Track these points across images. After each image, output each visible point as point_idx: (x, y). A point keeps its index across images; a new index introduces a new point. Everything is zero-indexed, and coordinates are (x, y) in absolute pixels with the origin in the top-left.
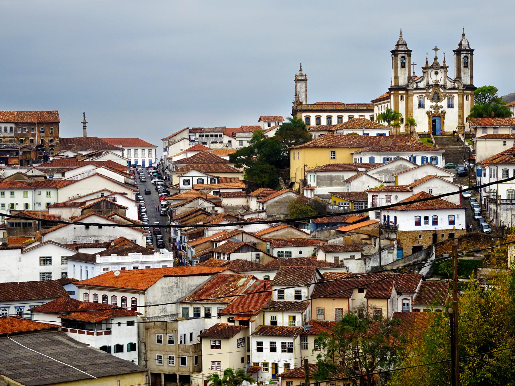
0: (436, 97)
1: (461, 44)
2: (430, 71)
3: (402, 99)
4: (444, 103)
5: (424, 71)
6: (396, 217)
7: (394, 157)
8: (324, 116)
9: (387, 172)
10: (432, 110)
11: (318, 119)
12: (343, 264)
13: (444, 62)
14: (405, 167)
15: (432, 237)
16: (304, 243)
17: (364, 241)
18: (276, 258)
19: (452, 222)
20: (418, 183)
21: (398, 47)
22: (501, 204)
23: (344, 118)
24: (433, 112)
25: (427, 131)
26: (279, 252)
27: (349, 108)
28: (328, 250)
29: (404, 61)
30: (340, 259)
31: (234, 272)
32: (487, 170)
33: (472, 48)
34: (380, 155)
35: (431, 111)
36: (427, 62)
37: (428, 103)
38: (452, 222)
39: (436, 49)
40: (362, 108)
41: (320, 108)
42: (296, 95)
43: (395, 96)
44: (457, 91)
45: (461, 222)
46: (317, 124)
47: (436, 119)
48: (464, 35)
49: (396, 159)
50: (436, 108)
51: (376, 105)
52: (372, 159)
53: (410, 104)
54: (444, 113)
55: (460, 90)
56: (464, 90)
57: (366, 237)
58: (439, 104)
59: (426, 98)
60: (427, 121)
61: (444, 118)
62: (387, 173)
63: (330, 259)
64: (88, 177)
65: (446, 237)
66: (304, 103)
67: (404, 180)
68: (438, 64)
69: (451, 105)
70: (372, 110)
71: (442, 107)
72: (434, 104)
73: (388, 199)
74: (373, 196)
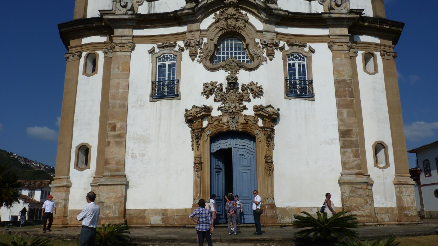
4: (270, 76)
10: (210, 102)
24: (216, 113)
35: (208, 110)
53: (113, 82)
58: (244, 77)
61: (270, 138)
71: (258, 92)
72: (220, 77)
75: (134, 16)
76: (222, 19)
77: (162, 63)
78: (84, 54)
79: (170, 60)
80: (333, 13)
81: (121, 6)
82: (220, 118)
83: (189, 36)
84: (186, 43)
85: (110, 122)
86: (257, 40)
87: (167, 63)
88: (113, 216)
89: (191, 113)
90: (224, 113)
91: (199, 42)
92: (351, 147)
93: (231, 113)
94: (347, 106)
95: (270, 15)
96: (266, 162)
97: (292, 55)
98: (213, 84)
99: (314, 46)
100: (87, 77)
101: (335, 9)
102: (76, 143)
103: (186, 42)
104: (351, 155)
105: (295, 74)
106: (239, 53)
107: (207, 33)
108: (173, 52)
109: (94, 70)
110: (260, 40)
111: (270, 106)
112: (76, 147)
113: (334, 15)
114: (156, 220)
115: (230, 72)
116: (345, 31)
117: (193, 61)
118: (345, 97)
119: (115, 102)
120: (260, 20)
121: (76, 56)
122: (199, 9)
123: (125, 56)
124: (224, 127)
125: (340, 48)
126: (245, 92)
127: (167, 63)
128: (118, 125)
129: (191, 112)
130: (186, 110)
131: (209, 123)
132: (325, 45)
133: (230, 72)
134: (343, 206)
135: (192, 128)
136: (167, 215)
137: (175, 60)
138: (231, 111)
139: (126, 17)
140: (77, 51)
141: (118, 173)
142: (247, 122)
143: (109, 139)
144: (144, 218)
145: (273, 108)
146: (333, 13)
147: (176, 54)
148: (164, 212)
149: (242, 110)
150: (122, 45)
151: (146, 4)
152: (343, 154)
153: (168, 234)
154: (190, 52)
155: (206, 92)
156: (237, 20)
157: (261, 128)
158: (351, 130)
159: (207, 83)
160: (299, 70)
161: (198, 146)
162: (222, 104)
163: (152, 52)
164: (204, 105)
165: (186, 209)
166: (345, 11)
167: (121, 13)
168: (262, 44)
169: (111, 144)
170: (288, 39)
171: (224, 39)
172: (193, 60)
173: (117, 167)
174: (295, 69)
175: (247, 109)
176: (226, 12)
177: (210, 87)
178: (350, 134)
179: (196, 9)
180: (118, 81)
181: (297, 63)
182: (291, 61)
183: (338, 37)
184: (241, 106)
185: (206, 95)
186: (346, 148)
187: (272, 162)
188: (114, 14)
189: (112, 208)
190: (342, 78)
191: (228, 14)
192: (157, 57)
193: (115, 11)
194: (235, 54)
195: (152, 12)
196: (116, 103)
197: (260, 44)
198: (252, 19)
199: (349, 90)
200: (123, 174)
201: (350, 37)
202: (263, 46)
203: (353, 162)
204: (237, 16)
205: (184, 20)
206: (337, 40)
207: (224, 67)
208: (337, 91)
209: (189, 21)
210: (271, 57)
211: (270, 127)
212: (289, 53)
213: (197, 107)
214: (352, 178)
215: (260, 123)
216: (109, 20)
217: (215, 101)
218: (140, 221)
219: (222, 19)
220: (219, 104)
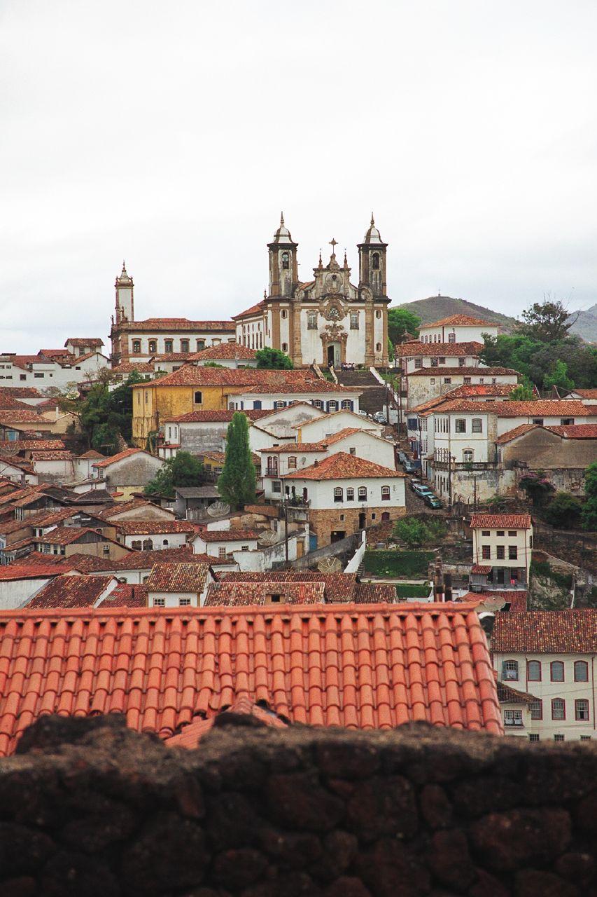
0: (334, 314)
1: (368, 235)
2: (325, 274)
3: (284, 315)
4: (346, 322)
5: (317, 274)
6: (305, 490)
7: (291, 400)
8: (177, 340)
9: (282, 423)
11: (169, 343)
12: (233, 559)
13: (346, 262)
14: (308, 417)
15: (358, 518)
16: (171, 529)
17: (259, 525)
18: (129, 550)
19: (386, 497)
20: (332, 438)
21: (277, 240)
22: (456, 471)
23: (190, 342)
24: (329, 335)
25: (322, 363)
26: (133, 543)
27: (197, 328)
28: (212, 538)
29: (287, 260)
30: (227, 552)
31: (82, 573)
32: (431, 420)
33: (384, 242)
34: (270, 398)
35: (327, 334)
36: (320, 261)
37: (322, 322)
38: (386, 497)
39: (334, 243)
40: (217, 328)
41: (154, 327)
42: (117, 308)
43: (273, 311)
44: (363, 305)
45: (398, 498)
46: (167, 350)
47: (333, 343)
48: (372, 222)
49: (292, 405)
50: (334, 328)
51: (239, 324)
52: (257, 404)
54: (345, 336)
55: (369, 302)
56: (373, 304)
57: (260, 518)
58: (338, 323)
59: (319, 314)
60: (321, 348)
62: (282, 424)
63: (214, 551)
64: (262, 430)
65: (379, 518)
66: (130, 319)
67: (312, 435)
68: (337, 265)
69: (355, 326)
70: (234, 332)
72: (331, 323)
73: (292, 463)
74: (269, 458)
116: (371, 305)
163: (307, 312)
198: (341, 302)
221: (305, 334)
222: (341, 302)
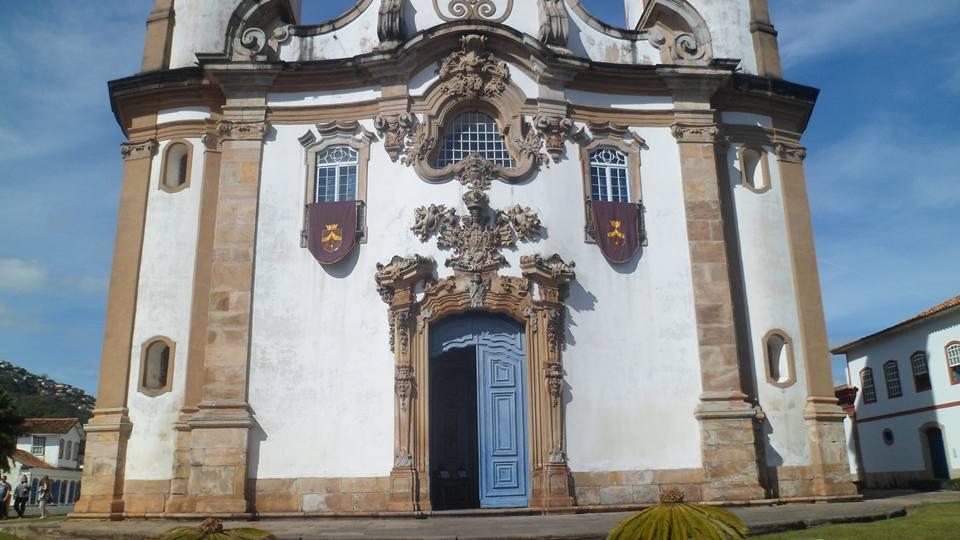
10: (429, 249)
24: (444, 273)
53: (223, 206)
58: (501, 196)
59: (378, 149)
72: (452, 195)
75: (269, 66)
76: (454, 74)
77: (327, 165)
78: (163, 144)
79: (346, 159)
80: (679, 67)
81: (242, 43)
82: (451, 283)
83: (385, 108)
84: (380, 123)
85: (217, 290)
86: (529, 119)
87: (338, 164)
88: (221, 493)
89: (389, 273)
90: (459, 273)
91: (407, 121)
92: (719, 344)
93: (473, 271)
94: (711, 258)
95: (553, 67)
96: (548, 376)
97: (599, 151)
98: (436, 210)
99: (643, 132)
100: (166, 194)
101: (682, 58)
102: (141, 337)
103: (378, 120)
104: (721, 359)
105: (604, 190)
106: (490, 146)
107: (425, 103)
108: (350, 141)
109: (183, 178)
110: (534, 119)
111: (556, 258)
112: (143, 345)
113: (681, 71)
114: (311, 502)
115: (471, 185)
116: (707, 106)
117: (394, 161)
118: (707, 238)
119: (226, 247)
120: (532, 78)
121: (146, 149)
122: (407, 53)
123: (250, 150)
124: (460, 303)
125: (695, 137)
126: (505, 227)
127: (338, 164)
128: (234, 297)
129: (387, 269)
130: (380, 266)
131: (427, 296)
132: (667, 132)
133: (471, 185)
134: (704, 465)
135: (390, 304)
136: (338, 491)
137: (355, 159)
138: (472, 267)
139: (250, 67)
140: (148, 138)
141: (231, 402)
142: (509, 291)
143: (213, 328)
144: (287, 497)
145: (561, 261)
146: (679, 67)
147: (358, 145)
148: (331, 486)
149: (496, 267)
150: (243, 126)
151: (295, 40)
152: (704, 356)
153: (342, 530)
154: (387, 141)
155: (420, 227)
156: (486, 77)
157: (537, 303)
158: (721, 306)
159: (423, 207)
160: (614, 181)
161: (403, 341)
162: (456, 253)
164: (417, 255)
165: (377, 478)
166: (704, 62)
167: (244, 58)
168: (538, 128)
169: (218, 338)
170: (591, 118)
171: (459, 115)
172: (394, 159)
173: (230, 387)
174: (605, 179)
175: (510, 266)
176: (463, 59)
177: (429, 216)
178: (717, 316)
179: (399, 53)
180: (233, 202)
181: (608, 166)
182: (597, 163)
183: (690, 115)
184: (498, 257)
185: (420, 233)
186: (711, 345)
187: (560, 377)
188: (229, 62)
189: (220, 476)
190: (700, 199)
191: (466, 64)
192: (317, 153)
193: (231, 54)
194: (482, 146)
195: (307, 59)
196: (228, 250)
197: (534, 128)
198: (517, 75)
199: (712, 224)
200: (244, 403)
201: (714, 113)
202: (540, 131)
203: (724, 373)
204: (484, 69)
205: (374, 76)
206: (688, 122)
207: (460, 175)
208: (690, 225)
209: (386, 77)
210: (556, 155)
211: (556, 300)
212: (593, 145)
213: (401, 260)
214: (722, 407)
215: (537, 294)
216: (217, 73)
217: (441, 246)
218: (279, 504)
219: (454, 74)
220: (449, 254)
221: (287, 274)
222: (517, 75)
